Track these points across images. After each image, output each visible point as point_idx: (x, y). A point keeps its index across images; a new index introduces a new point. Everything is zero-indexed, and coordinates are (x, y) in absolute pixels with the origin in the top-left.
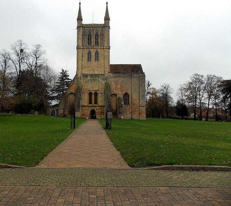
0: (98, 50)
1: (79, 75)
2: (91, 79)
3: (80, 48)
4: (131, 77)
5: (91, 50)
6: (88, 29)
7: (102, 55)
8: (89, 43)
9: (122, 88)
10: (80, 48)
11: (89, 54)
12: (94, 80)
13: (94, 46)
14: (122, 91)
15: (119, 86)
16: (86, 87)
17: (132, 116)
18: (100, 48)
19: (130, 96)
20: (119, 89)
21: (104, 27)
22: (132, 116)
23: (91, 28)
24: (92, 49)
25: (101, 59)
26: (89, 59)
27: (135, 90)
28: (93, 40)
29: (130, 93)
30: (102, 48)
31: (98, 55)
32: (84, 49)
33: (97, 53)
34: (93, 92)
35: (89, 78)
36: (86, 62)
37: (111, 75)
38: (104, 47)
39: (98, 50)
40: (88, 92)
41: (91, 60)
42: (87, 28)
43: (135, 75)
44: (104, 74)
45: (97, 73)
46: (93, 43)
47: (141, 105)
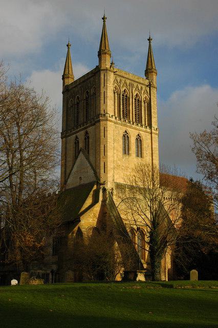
0: (141, 132)
1: (109, 183)
3: (111, 121)
5: (130, 130)
6: (123, 82)
7: (148, 146)
10: (111, 121)
11: (126, 137)
13: (133, 123)
21: (150, 86)
24: (130, 127)
25: (147, 154)
26: (126, 151)
28: (132, 108)
33: (139, 140)
39: (141, 132)
42: (122, 78)
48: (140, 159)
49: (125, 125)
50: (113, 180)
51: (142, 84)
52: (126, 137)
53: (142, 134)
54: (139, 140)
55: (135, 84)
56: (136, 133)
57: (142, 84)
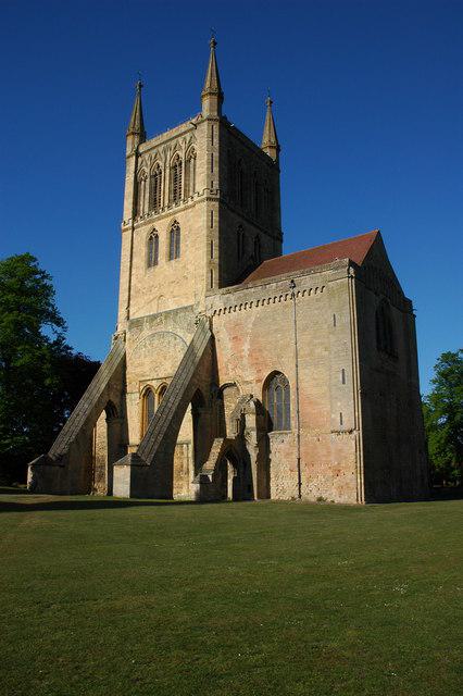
2: (153, 335)
4: (293, 295)
8: (154, 203)
9: (260, 351)
11: (153, 239)
12: (162, 335)
14: (257, 365)
15: (246, 347)
16: (138, 370)
17: (300, 484)
18: (182, 206)
19: (292, 384)
20: (245, 361)
22: (300, 484)
23: (161, 149)
27: (311, 353)
29: (289, 374)
30: (190, 203)
31: (178, 234)
32: (138, 227)
33: (175, 231)
34: (155, 385)
35: (146, 332)
36: (142, 272)
37: (218, 300)
38: (196, 199)
40: (142, 388)
41: (156, 263)
43: (306, 281)
44: (192, 306)
45: (172, 306)
46: (165, 198)
47: (338, 427)
48: (173, 262)
49: (149, 222)
50: (128, 318)
51: (185, 132)
52: (153, 239)
53: (180, 217)
54: (175, 231)
55: (173, 143)
56: (168, 220)
57: (185, 132)
